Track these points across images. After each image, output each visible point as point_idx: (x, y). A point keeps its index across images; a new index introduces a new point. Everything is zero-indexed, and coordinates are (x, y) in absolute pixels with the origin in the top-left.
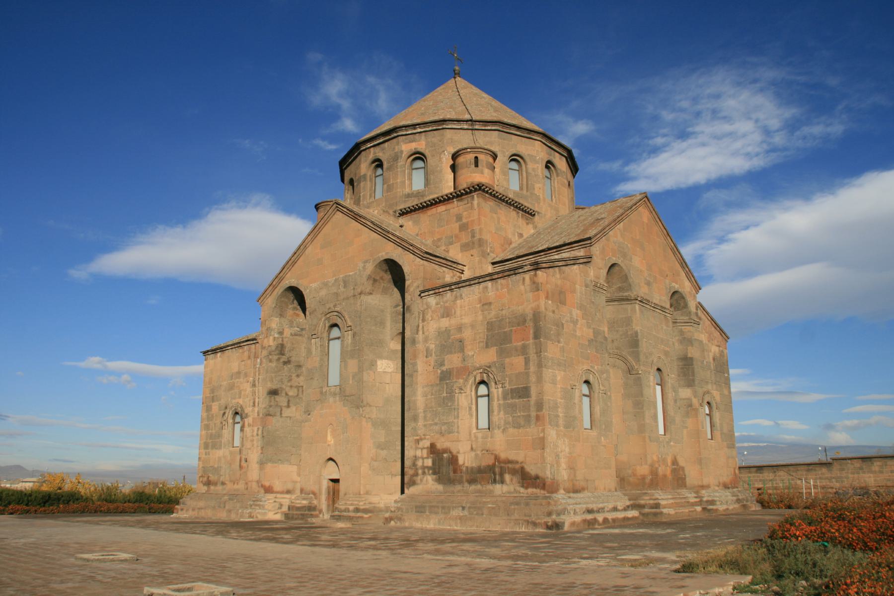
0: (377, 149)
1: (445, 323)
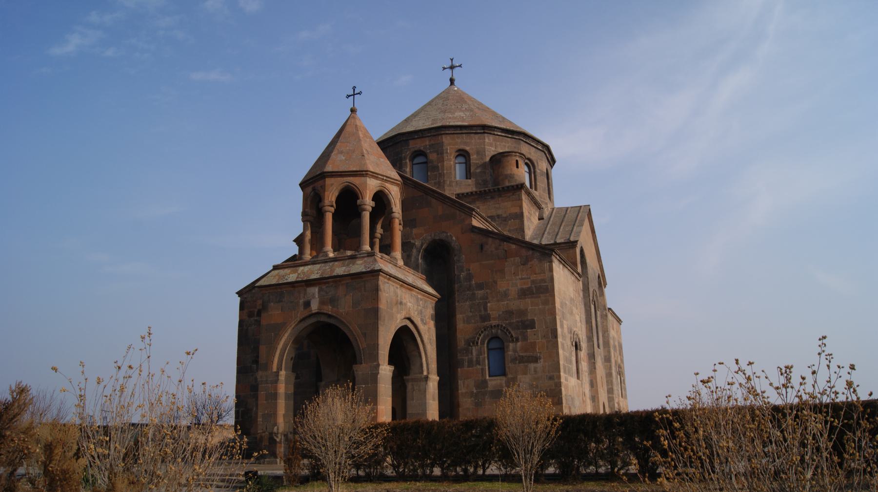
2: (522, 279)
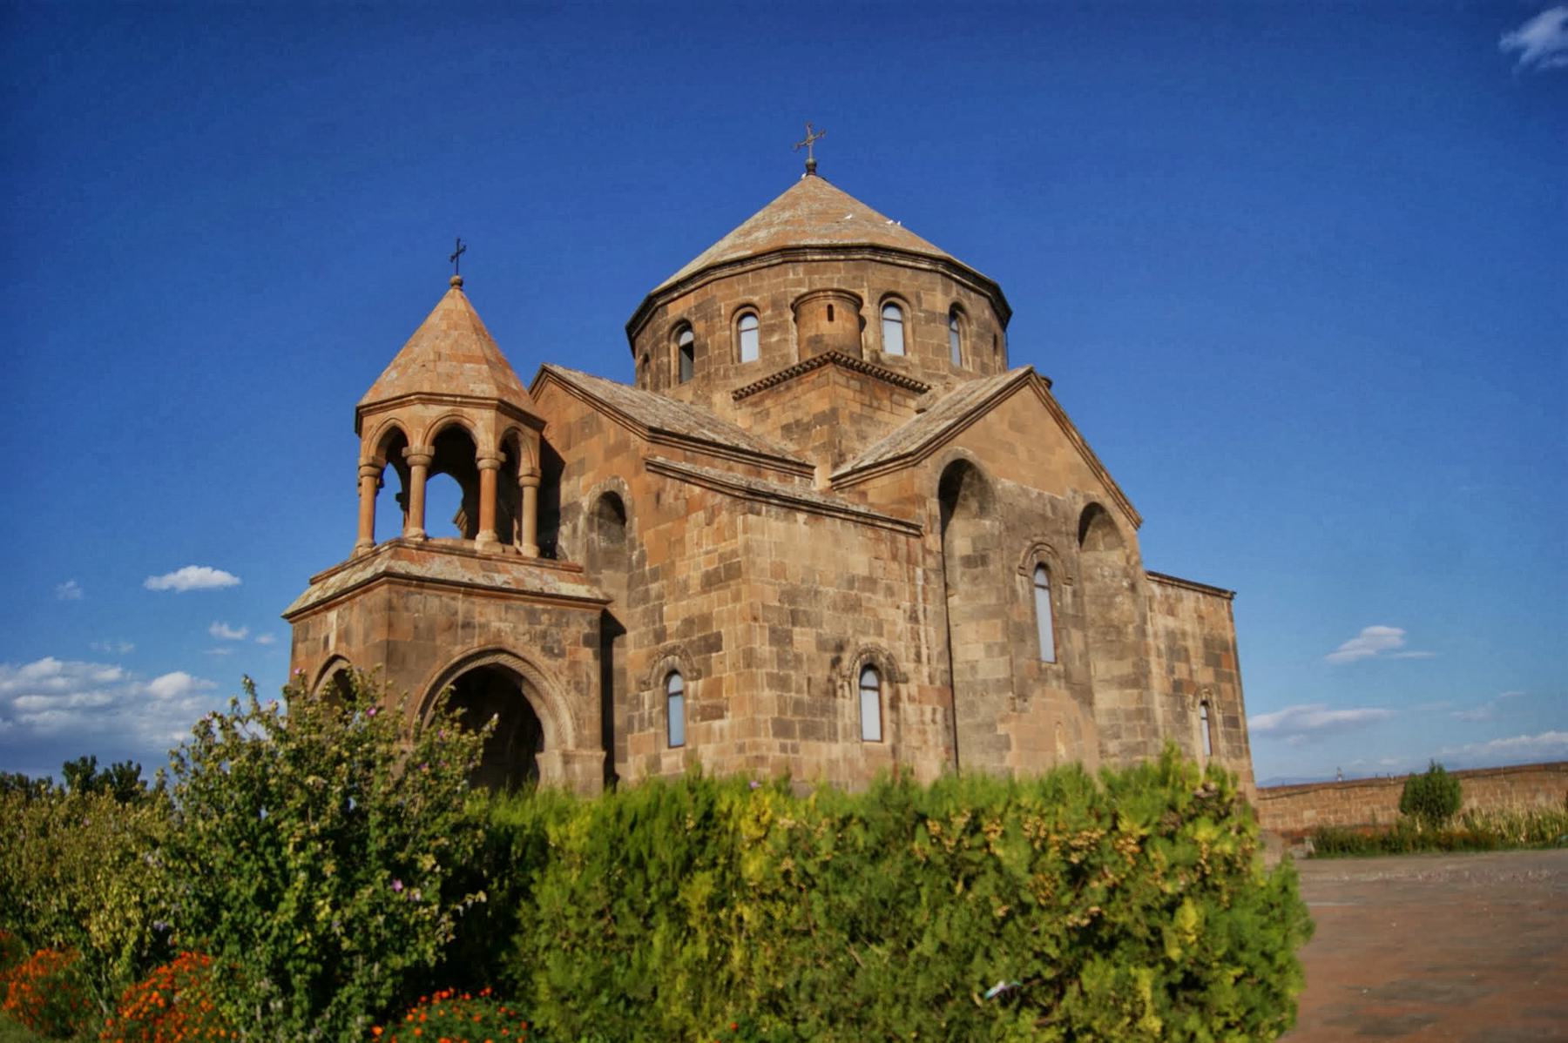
0: (962, 291)
1: (1171, 622)
2: (707, 553)
